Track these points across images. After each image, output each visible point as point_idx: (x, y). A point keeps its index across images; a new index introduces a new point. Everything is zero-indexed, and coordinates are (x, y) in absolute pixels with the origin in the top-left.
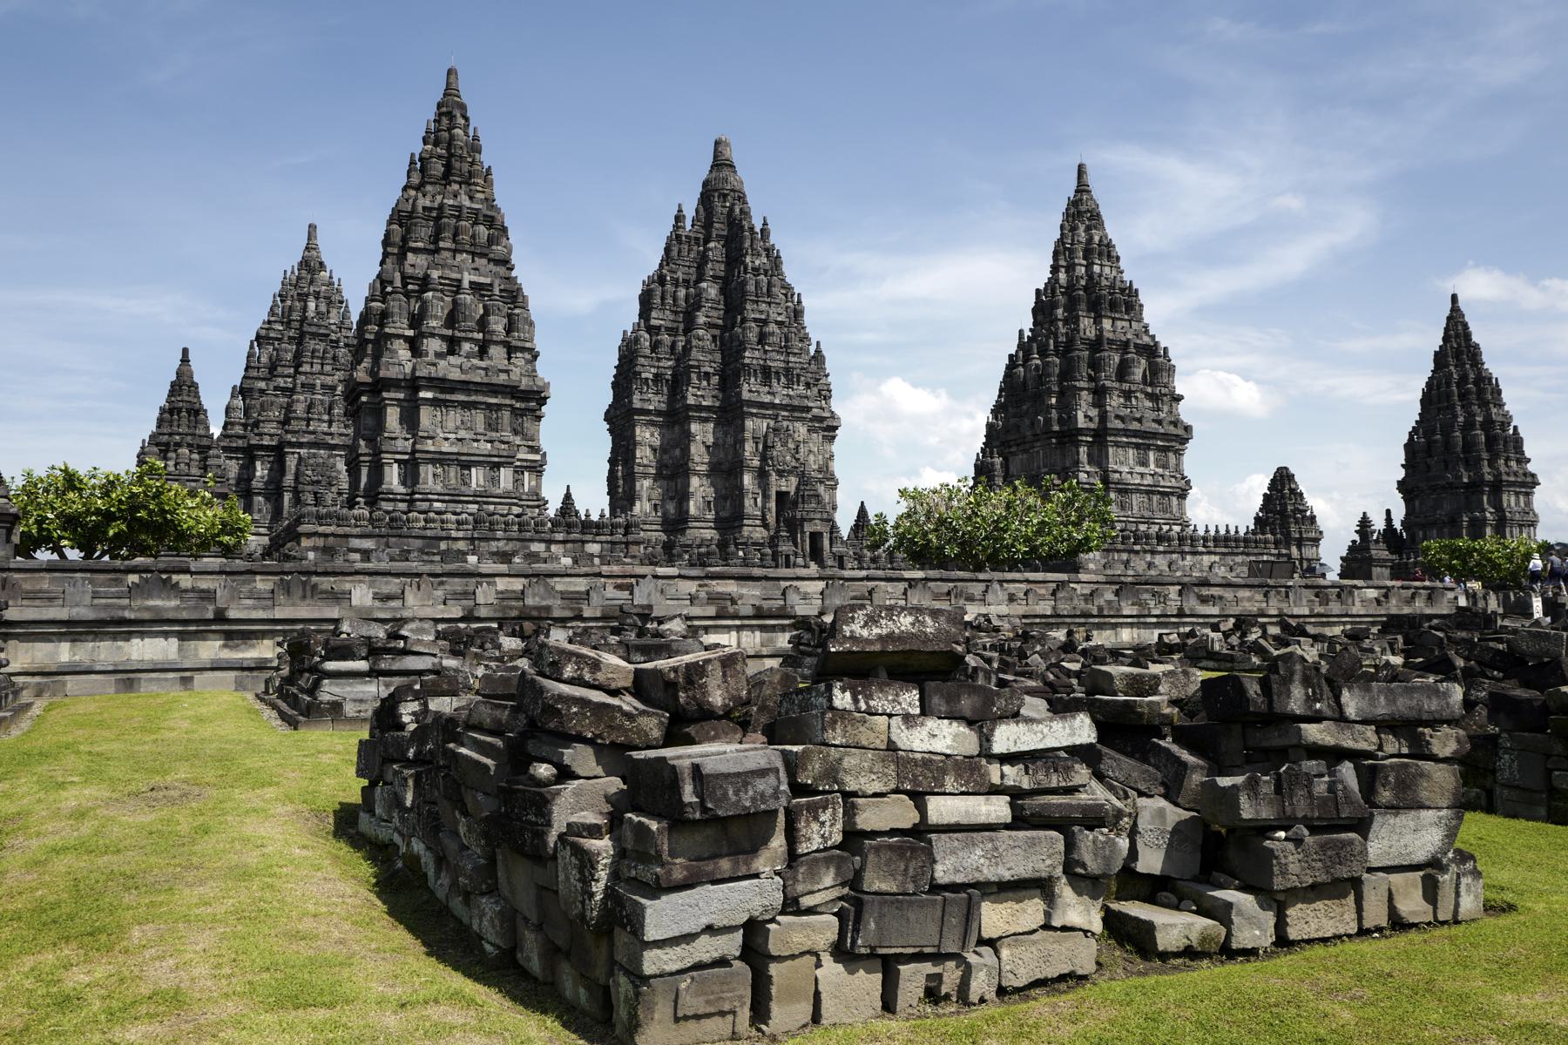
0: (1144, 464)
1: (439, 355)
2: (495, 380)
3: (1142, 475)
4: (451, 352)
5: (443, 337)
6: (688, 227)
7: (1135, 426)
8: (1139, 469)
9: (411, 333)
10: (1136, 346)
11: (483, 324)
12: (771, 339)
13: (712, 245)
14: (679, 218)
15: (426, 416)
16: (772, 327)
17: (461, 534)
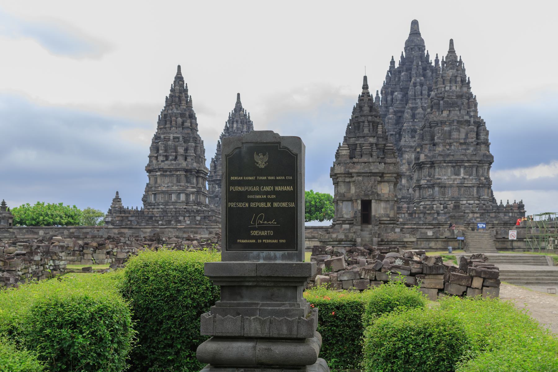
0: (458, 174)
1: (163, 161)
2: (178, 167)
3: (455, 179)
4: (167, 160)
5: (163, 156)
6: (397, 65)
7: (451, 158)
8: (453, 177)
9: (156, 155)
10: (458, 122)
11: (176, 151)
12: (418, 116)
13: (403, 74)
14: (393, 62)
15: (159, 181)
16: (420, 110)
17: (158, 215)
